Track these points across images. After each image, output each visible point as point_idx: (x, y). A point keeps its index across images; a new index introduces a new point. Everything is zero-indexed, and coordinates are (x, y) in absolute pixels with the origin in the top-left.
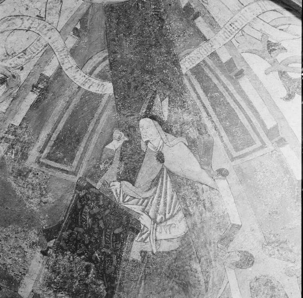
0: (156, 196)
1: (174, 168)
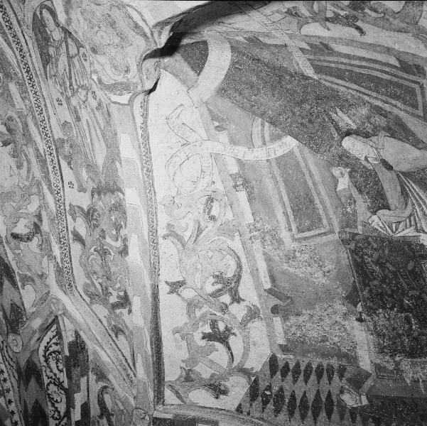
0: (417, 207)
1: (405, 167)
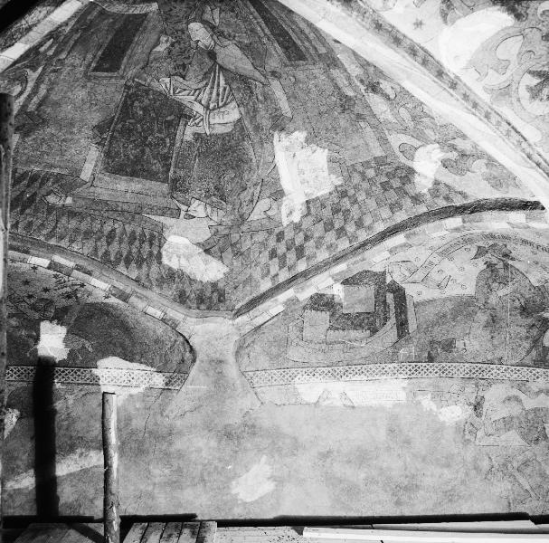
0: (208, 88)
